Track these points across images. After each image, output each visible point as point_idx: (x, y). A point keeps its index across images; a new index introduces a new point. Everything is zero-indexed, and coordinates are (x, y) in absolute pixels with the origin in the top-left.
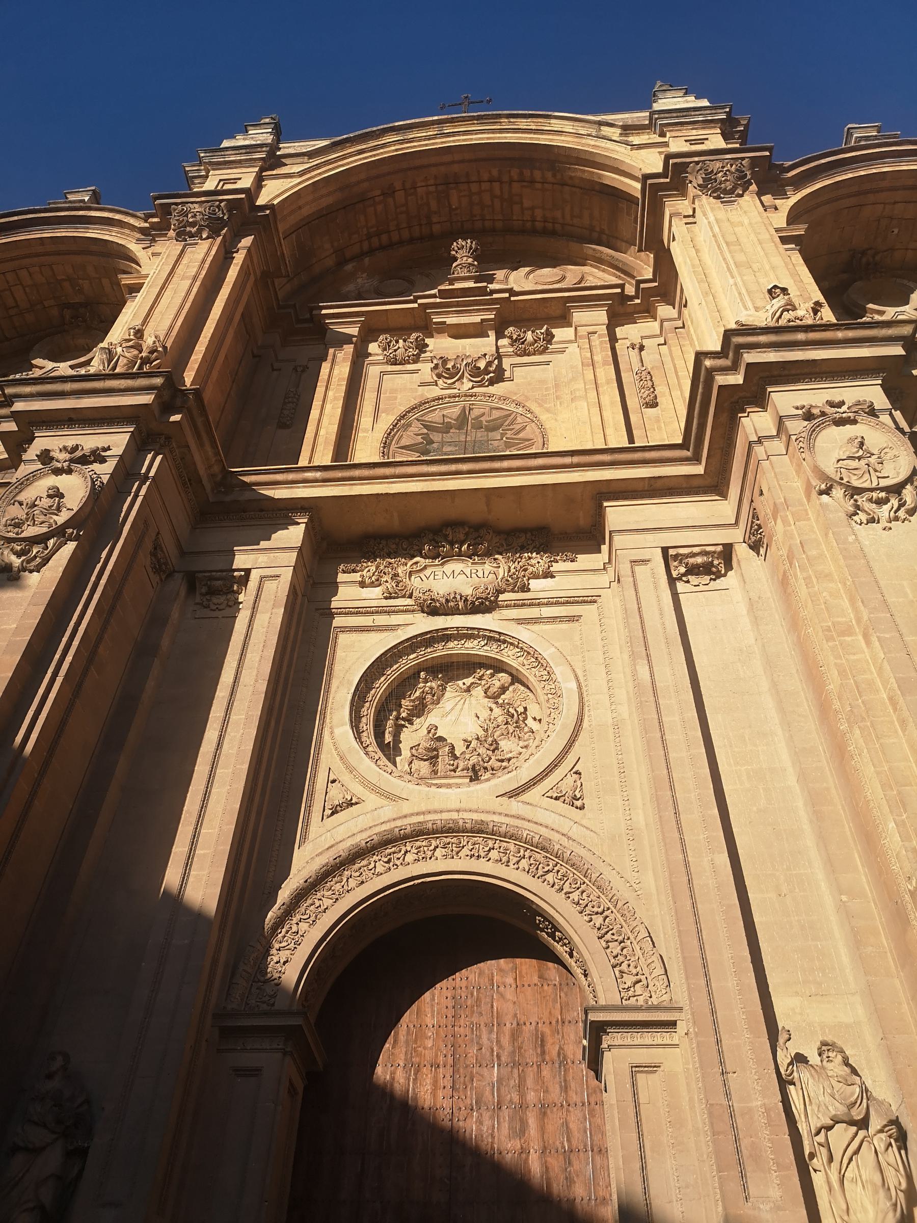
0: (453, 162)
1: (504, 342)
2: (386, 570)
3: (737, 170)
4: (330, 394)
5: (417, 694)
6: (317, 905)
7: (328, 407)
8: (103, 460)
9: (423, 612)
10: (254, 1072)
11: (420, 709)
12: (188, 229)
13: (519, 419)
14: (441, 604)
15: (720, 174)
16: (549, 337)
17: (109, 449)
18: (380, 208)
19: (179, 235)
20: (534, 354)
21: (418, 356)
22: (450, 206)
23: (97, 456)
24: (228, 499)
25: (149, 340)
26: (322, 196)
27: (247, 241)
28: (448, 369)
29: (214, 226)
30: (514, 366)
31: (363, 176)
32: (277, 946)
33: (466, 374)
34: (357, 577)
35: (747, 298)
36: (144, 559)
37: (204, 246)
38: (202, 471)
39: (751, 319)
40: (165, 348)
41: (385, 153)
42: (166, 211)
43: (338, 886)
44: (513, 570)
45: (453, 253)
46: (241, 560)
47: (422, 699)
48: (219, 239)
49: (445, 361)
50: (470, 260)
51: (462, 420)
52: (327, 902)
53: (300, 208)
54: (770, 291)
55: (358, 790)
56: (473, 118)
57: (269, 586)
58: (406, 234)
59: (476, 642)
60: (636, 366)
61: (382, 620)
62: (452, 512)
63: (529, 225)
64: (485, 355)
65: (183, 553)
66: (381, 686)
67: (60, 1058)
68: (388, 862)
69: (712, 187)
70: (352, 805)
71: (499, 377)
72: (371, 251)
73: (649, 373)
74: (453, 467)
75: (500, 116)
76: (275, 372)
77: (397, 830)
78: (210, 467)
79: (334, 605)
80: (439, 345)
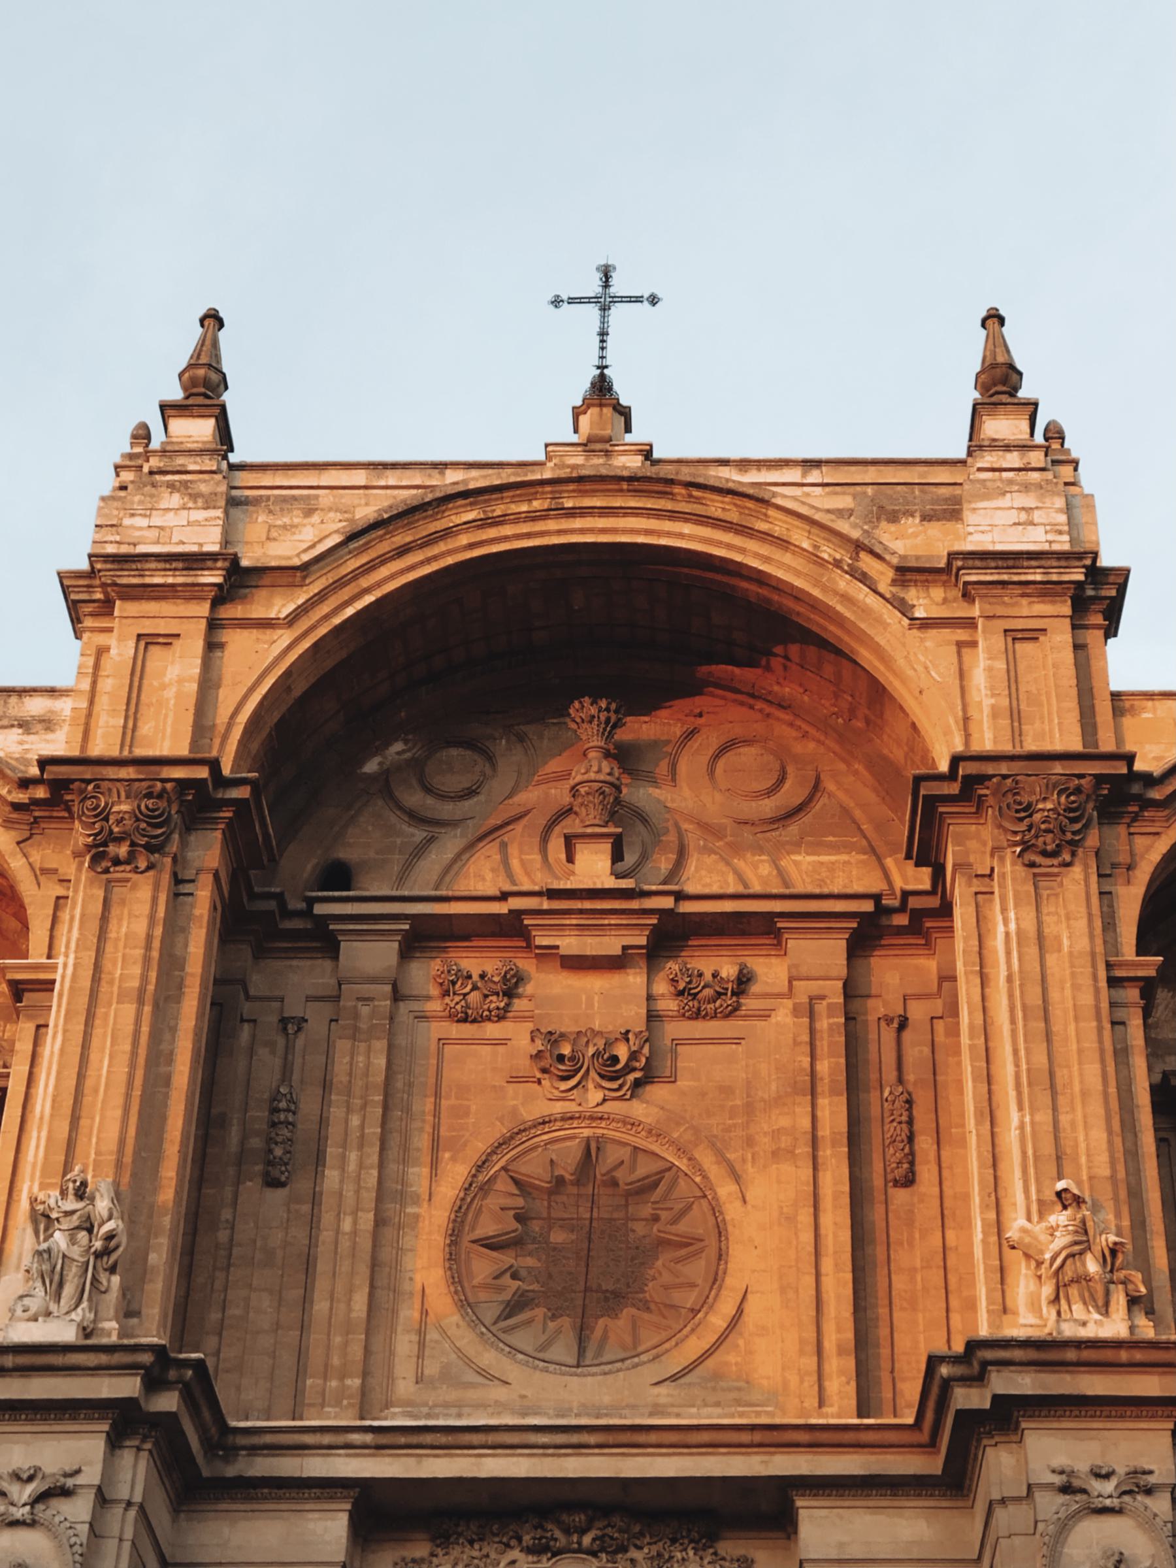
3: (1068, 810)
4: (355, 1121)
7: (353, 1156)
15: (1037, 817)
16: (744, 980)
20: (714, 1017)
21: (506, 1009)
28: (561, 1058)
30: (677, 1042)
33: (593, 1074)
35: (1032, 1171)
39: (1027, 1240)
41: (450, 552)
54: (1059, 1194)
60: (890, 1075)
64: (628, 1032)
69: (1022, 842)
73: (909, 1102)
74: (575, 1438)
75: (671, 482)
76: (246, 1026)
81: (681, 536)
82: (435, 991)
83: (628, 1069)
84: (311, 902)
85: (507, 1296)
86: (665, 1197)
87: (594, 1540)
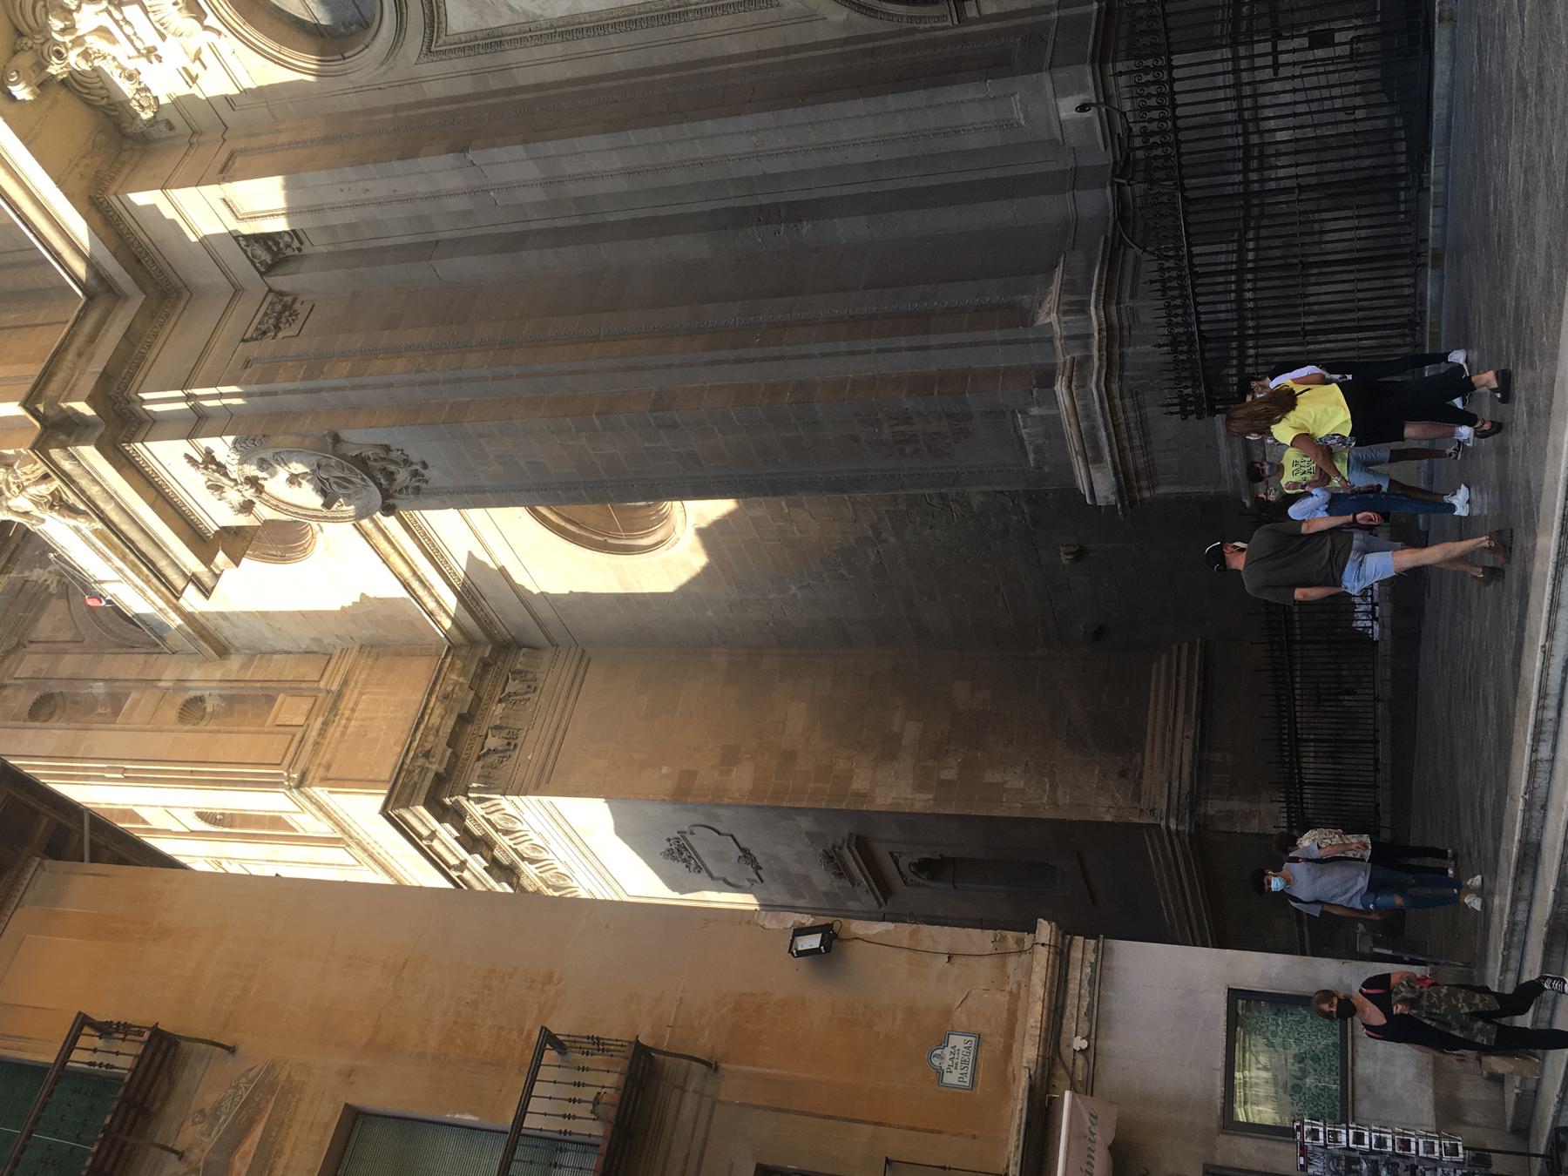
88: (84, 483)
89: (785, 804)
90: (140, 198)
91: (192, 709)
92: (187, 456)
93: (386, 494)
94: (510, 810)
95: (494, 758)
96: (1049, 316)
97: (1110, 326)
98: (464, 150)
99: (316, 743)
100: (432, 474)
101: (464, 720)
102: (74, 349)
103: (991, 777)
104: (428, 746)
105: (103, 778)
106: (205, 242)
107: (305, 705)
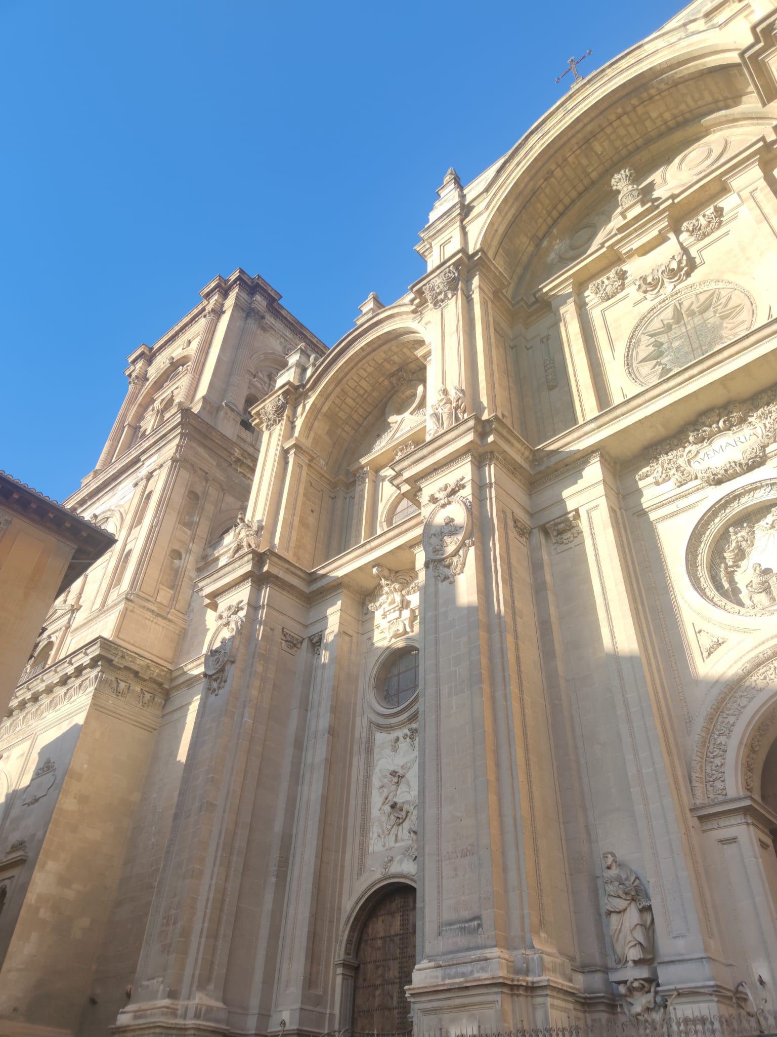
0: (585, 126)
1: (684, 236)
2: (670, 466)
5: (734, 545)
6: (727, 721)
8: (463, 487)
9: (710, 485)
10: (734, 840)
11: (741, 554)
12: (439, 298)
13: (723, 293)
14: (722, 475)
16: (719, 212)
17: (463, 478)
18: (547, 190)
19: (435, 305)
20: (713, 232)
21: (623, 284)
22: (596, 154)
23: (460, 486)
24: (542, 468)
25: (453, 395)
26: (507, 213)
27: (476, 281)
28: (650, 284)
29: (452, 285)
30: (700, 251)
31: (527, 179)
32: (711, 756)
33: (665, 280)
34: (650, 480)
36: (513, 534)
37: (452, 303)
38: (519, 459)
40: (462, 391)
42: (420, 293)
43: (735, 706)
44: (768, 426)
45: (614, 188)
46: (571, 505)
47: (739, 547)
48: (459, 292)
49: (644, 279)
50: (630, 187)
51: (678, 316)
52: (732, 719)
53: (496, 231)
55: (721, 634)
56: (585, 85)
57: (594, 514)
58: (573, 194)
59: (762, 490)
61: (682, 503)
62: (701, 405)
63: (663, 128)
65: (531, 515)
66: (704, 550)
67: (610, 856)
68: (765, 678)
70: (719, 644)
71: (692, 265)
72: (555, 222)
74: (687, 375)
75: (604, 70)
76: (530, 351)
77: (761, 655)
78: (523, 454)
79: (644, 506)
80: (636, 268)
81: (616, 83)
82: (592, 296)
83: (680, 269)
84: (534, 295)
85: (660, 371)
86: (718, 299)
87: (724, 422)
88: (239, 562)
89: (50, 826)
90: (339, 603)
91: (177, 554)
92: (242, 601)
93: (210, 676)
94: (89, 690)
95: (115, 685)
96: (200, 999)
97: (186, 1029)
98: (329, 732)
99: (144, 607)
100: (212, 697)
101: (136, 674)
102: (289, 567)
103: (34, 936)
104: (127, 657)
105: (155, 517)
106: (326, 618)
107: (165, 602)
